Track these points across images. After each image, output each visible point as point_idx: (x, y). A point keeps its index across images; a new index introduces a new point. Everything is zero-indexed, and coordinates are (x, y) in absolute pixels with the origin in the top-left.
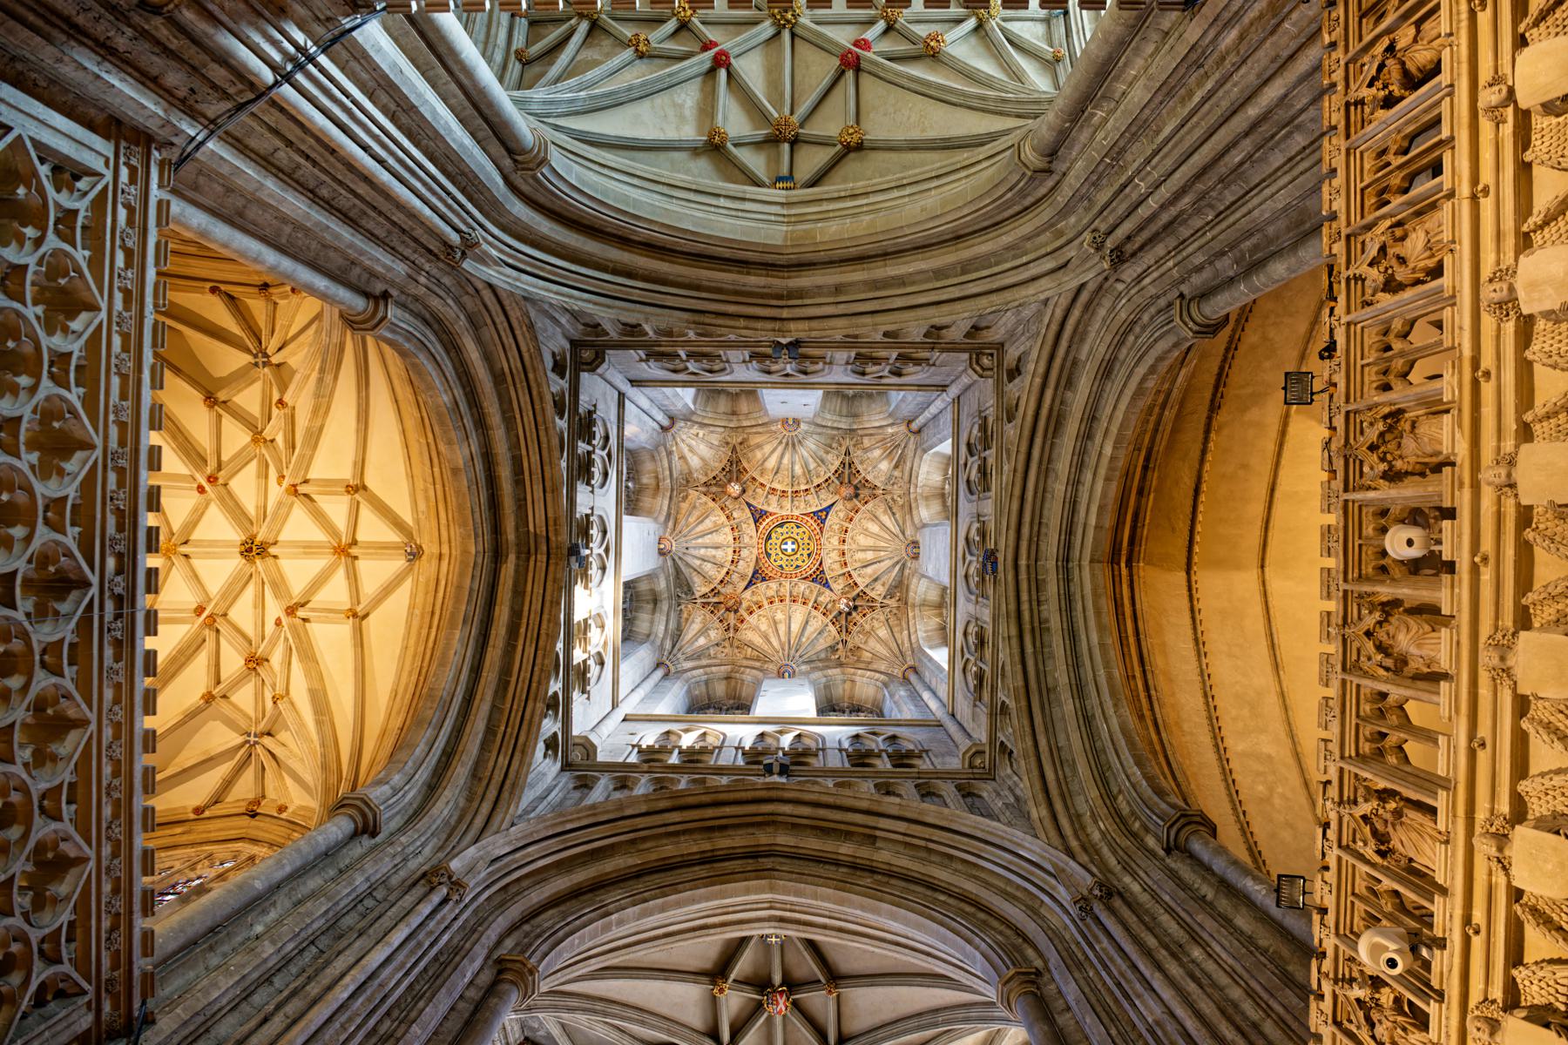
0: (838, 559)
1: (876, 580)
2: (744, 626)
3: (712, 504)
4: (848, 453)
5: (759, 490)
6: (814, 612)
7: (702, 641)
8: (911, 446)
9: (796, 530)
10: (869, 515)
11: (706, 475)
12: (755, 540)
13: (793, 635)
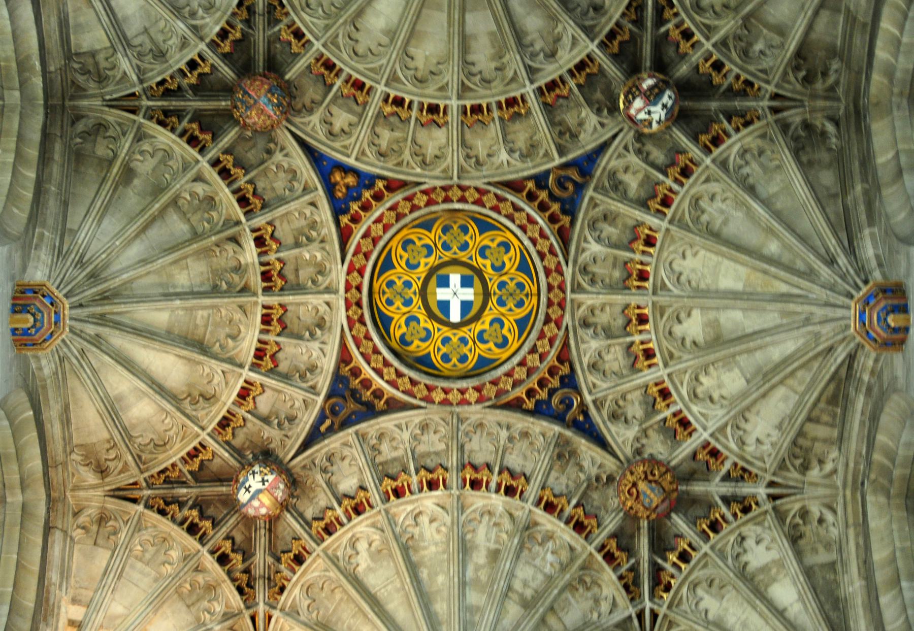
0: (494, 129)
2: (729, 445)
4: (128, 104)
5: (264, 403)
6: (681, 202)
9: (398, 273)
10: (340, 28)
11: (211, 588)
12: (434, 413)
13: (758, 282)
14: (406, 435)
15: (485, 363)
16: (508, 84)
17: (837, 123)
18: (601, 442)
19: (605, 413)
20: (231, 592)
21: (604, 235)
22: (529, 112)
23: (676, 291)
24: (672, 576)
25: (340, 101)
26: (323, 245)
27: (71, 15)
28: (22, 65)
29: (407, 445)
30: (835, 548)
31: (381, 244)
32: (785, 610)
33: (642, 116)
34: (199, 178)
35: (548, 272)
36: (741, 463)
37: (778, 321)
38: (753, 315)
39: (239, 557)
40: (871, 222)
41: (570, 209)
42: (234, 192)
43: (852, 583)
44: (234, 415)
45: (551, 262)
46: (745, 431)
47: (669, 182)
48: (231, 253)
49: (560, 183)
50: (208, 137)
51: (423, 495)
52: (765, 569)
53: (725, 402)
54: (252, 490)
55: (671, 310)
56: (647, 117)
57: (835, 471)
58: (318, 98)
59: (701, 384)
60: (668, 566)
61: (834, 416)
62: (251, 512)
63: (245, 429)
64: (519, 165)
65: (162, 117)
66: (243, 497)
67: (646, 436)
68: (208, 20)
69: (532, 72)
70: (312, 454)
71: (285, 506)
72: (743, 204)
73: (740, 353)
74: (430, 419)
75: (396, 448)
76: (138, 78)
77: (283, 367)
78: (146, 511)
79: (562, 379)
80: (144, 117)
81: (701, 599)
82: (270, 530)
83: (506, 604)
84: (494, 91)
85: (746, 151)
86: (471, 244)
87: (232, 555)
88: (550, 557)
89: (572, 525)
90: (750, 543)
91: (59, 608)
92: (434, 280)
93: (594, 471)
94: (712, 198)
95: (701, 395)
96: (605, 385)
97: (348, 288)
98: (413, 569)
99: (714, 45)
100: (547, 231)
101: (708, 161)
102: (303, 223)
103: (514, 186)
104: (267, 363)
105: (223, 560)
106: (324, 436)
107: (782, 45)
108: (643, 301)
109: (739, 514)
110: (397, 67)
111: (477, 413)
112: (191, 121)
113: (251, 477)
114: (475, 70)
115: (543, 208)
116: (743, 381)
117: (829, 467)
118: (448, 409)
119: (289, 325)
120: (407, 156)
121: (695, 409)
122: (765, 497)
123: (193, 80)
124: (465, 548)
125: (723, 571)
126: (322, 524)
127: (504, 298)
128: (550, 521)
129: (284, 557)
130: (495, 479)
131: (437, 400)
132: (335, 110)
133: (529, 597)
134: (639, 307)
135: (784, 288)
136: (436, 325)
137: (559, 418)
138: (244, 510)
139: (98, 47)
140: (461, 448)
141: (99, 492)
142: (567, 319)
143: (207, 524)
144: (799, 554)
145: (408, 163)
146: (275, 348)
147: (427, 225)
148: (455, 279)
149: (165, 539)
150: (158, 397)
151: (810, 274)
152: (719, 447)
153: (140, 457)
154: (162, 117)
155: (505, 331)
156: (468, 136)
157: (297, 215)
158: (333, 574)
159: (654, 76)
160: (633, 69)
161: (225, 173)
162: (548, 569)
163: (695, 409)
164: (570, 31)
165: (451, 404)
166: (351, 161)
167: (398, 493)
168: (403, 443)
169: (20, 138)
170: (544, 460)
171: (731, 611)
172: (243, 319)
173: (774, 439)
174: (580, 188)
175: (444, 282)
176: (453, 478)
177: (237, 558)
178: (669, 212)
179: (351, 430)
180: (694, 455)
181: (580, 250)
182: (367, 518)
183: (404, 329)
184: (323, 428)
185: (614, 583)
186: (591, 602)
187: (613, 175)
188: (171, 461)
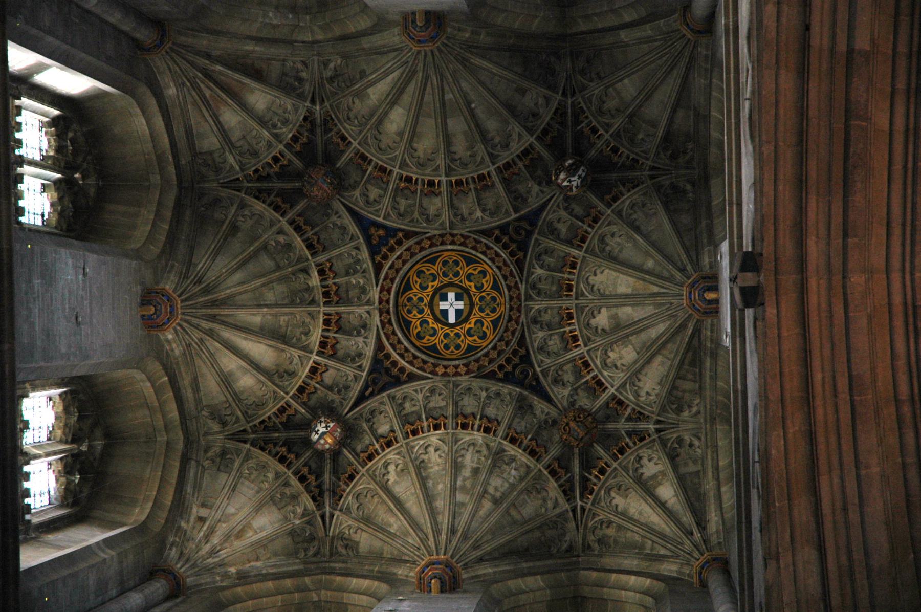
0: (472, 196)
1: (511, 109)
2: (628, 396)
3: (362, 484)
4: (234, 184)
5: (328, 377)
6: (593, 241)
7: (667, 492)
8: (203, 42)
11: (294, 498)
14: (420, 396)
15: (470, 349)
16: (478, 166)
17: (693, 185)
18: (548, 399)
19: (549, 378)
20: (307, 500)
21: (546, 262)
22: (493, 185)
23: (590, 297)
24: (595, 485)
25: (373, 181)
26: (364, 274)
27: (194, 127)
28: (160, 158)
29: (421, 403)
30: (700, 462)
31: (401, 273)
32: (666, 502)
33: (565, 183)
34: (281, 232)
35: (509, 289)
36: (638, 409)
37: (653, 312)
38: (639, 308)
39: (313, 478)
40: (709, 244)
41: (523, 247)
42: (304, 241)
43: (708, 483)
44: (308, 385)
45: (511, 282)
46: (639, 387)
47: (585, 227)
48: (303, 280)
49: (517, 231)
50: (288, 206)
51: (430, 433)
52: (654, 477)
53: (625, 368)
54: (319, 432)
55: (588, 308)
56: (568, 184)
57: (698, 413)
58: (358, 179)
59: (609, 357)
60: (591, 477)
61: (695, 374)
62: (319, 447)
63: (316, 395)
64: (489, 219)
65: (257, 194)
66: (315, 437)
67: (577, 394)
68: (284, 130)
69: (493, 158)
70: (361, 410)
71: (342, 443)
72: (630, 238)
73: (632, 335)
74: (436, 386)
75: (415, 405)
76: (240, 168)
77: (340, 353)
78: (251, 448)
79: (521, 357)
80: (245, 194)
81: (614, 498)
82: (334, 460)
83: (483, 501)
84: (469, 170)
85: (634, 205)
86: (461, 273)
87: (309, 476)
88: (513, 472)
89: (528, 451)
90: (645, 461)
91: (191, 508)
92: (437, 297)
93: (543, 417)
94: (613, 235)
95: (610, 365)
96: (549, 361)
97: (381, 302)
98: (423, 481)
99: (611, 136)
100: (509, 262)
101: (609, 212)
102: (351, 261)
103: (487, 233)
104: (329, 351)
105: (302, 479)
106: (367, 398)
107: (656, 133)
108: (570, 304)
109: (638, 442)
110: (406, 155)
111: (466, 381)
112: (276, 196)
113: (319, 425)
114: (457, 157)
115: (505, 247)
116: (635, 353)
117: (695, 409)
118: (448, 379)
119: (343, 326)
120: (416, 215)
121: (606, 373)
122: (653, 430)
123: (277, 170)
124: (456, 467)
125: (625, 479)
126: (366, 454)
127: (483, 307)
128: (513, 449)
129: (343, 477)
130: (477, 422)
131: (440, 373)
132: (370, 187)
133: (499, 498)
134: (568, 309)
135: (655, 289)
136: (440, 325)
137: (520, 384)
138: (315, 447)
139: (213, 148)
140: (456, 404)
141: (221, 437)
142: (523, 318)
143: (292, 456)
144: (675, 467)
145: (418, 220)
146: (334, 342)
147: (433, 261)
148: (451, 296)
149: (264, 467)
150: (255, 372)
151: (671, 279)
152: (622, 398)
153: (246, 413)
154: (257, 194)
155: (484, 329)
156: (455, 201)
157: (346, 255)
158: (373, 486)
159: (573, 158)
160: (561, 156)
161: (298, 229)
162: (512, 480)
163: (606, 373)
164: (517, 130)
165: (449, 375)
166: (381, 220)
167: (415, 433)
168: (418, 401)
169: (160, 203)
170: (510, 409)
171: (632, 505)
172: (312, 322)
173: (657, 392)
174: (529, 234)
175: (444, 298)
176: (450, 422)
177: (312, 478)
178: (585, 246)
179: (384, 394)
180: (607, 404)
181: (530, 274)
182: (394, 450)
183: (419, 329)
184: (367, 393)
185: (555, 488)
186: (540, 502)
187: (550, 224)
188: (267, 415)
